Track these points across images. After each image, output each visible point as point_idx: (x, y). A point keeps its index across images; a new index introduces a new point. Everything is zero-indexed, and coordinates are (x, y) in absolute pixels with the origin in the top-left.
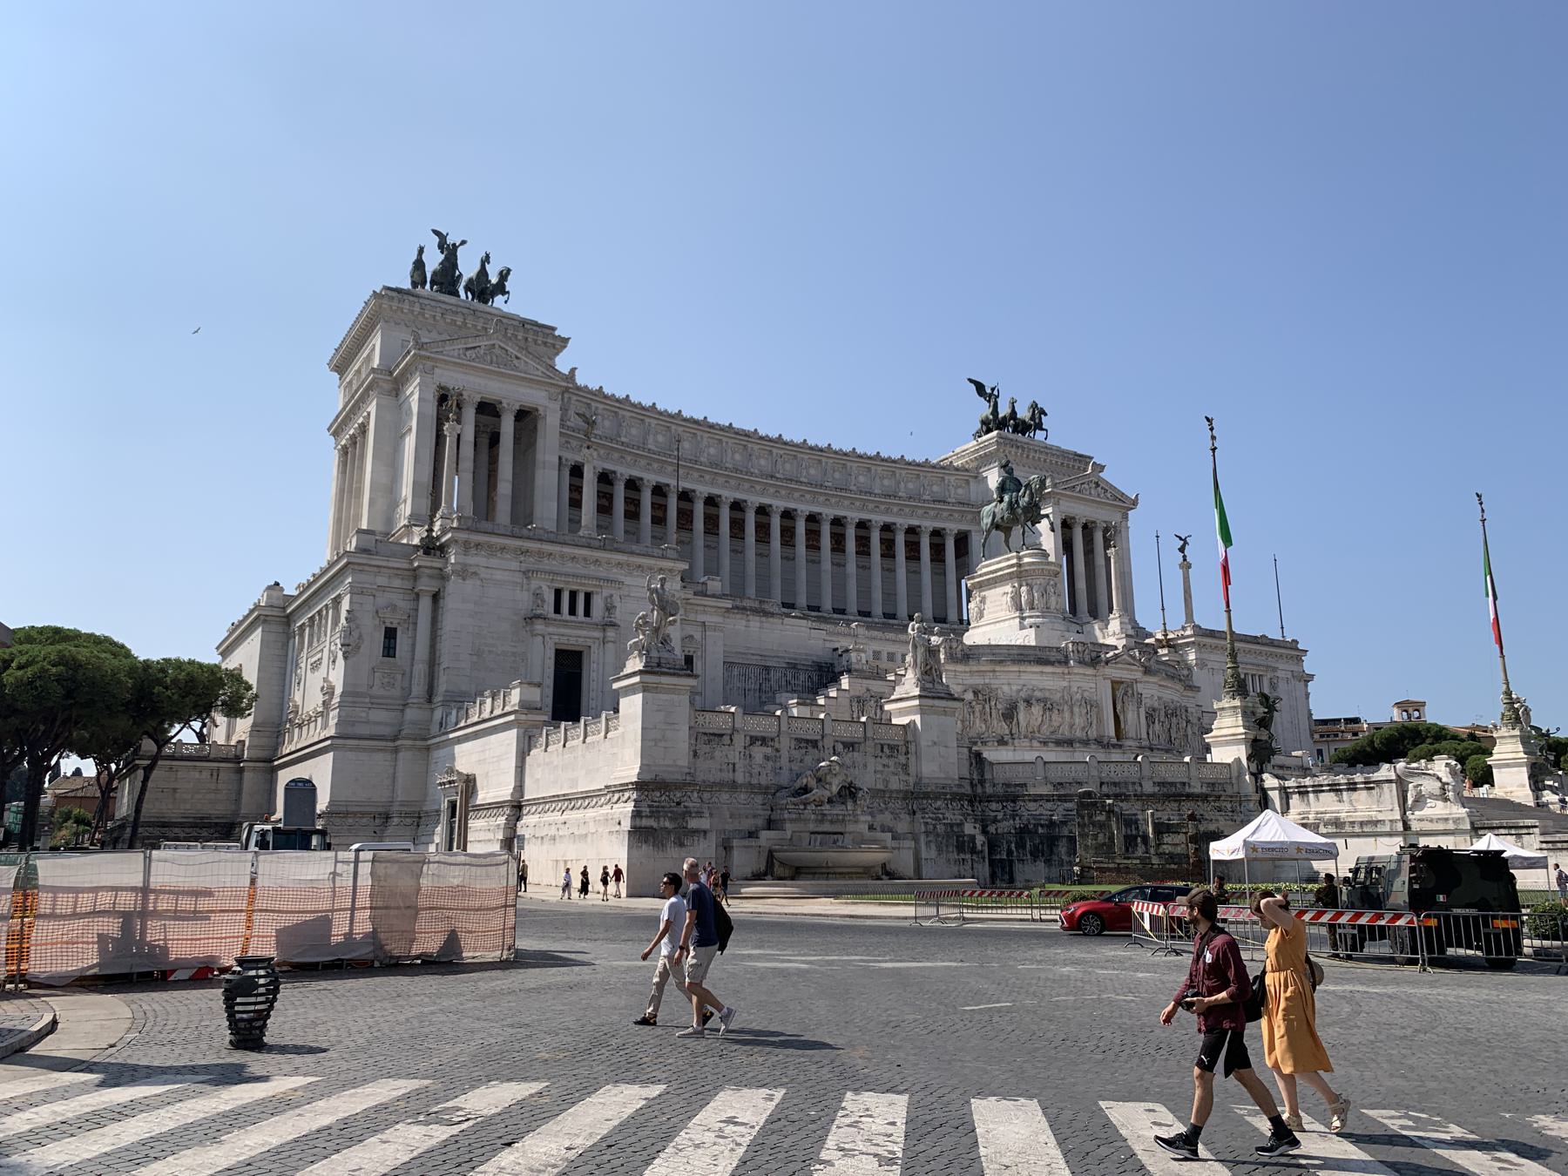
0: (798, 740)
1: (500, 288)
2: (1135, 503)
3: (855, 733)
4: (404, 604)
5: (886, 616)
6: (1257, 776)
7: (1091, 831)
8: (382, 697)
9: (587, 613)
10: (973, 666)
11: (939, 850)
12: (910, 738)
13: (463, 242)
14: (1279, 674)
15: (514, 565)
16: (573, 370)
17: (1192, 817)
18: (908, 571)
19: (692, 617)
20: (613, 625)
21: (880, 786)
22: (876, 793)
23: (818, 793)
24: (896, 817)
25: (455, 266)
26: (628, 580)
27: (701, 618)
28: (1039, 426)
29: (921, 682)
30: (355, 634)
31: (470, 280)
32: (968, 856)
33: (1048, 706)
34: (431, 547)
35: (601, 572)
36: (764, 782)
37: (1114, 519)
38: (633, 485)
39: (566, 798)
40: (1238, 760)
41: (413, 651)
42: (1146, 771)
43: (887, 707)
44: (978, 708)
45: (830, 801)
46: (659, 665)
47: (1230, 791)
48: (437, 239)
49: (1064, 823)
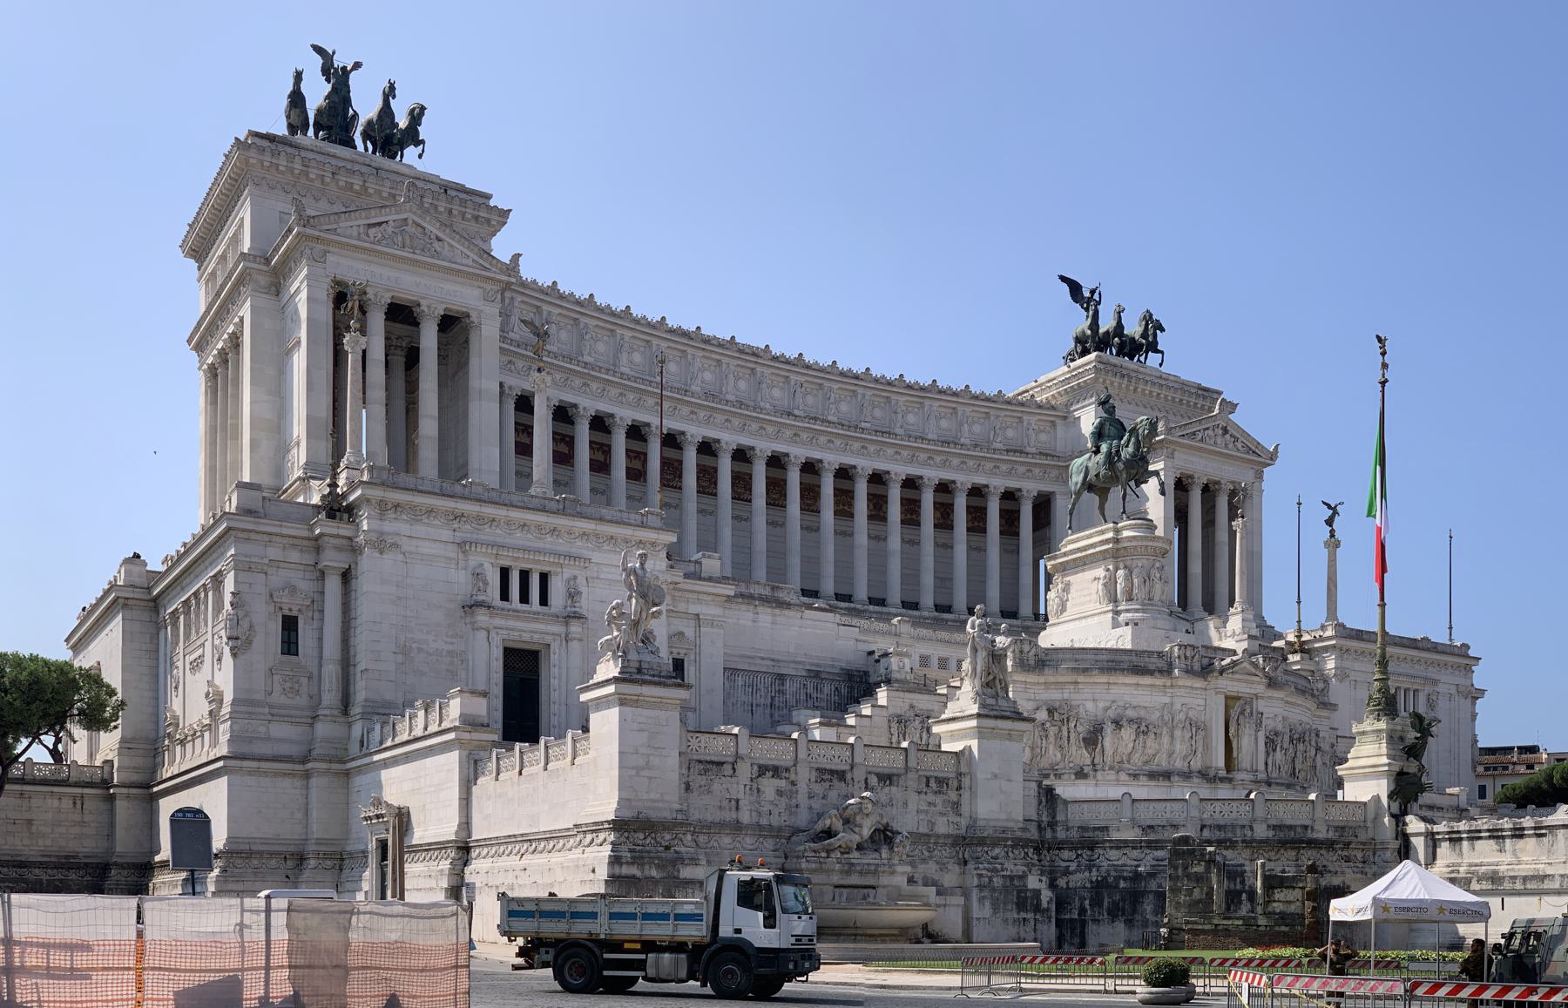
2: (1273, 456)
3: (893, 762)
4: (305, 585)
5: (938, 608)
6: (1399, 818)
7: (1185, 884)
8: (281, 707)
10: (1049, 676)
11: (995, 909)
12: (963, 769)
15: (446, 534)
17: (1312, 869)
18: (970, 548)
19: (681, 607)
20: (578, 617)
22: (917, 838)
23: (844, 838)
24: (943, 867)
26: (596, 557)
29: (980, 696)
30: (245, 624)
32: (1030, 916)
35: (562, 545)
36: (775, 821)
37: (1244, 477)
38: (600, 423)
39: (527, 839)
40: (1377, 799)
41: (321, 648)
42: (1260, 812)
43: (936, 729)
44: (1052, 731)
45: (860, 847)
47: (1362, 837)
49: (1152, 875)
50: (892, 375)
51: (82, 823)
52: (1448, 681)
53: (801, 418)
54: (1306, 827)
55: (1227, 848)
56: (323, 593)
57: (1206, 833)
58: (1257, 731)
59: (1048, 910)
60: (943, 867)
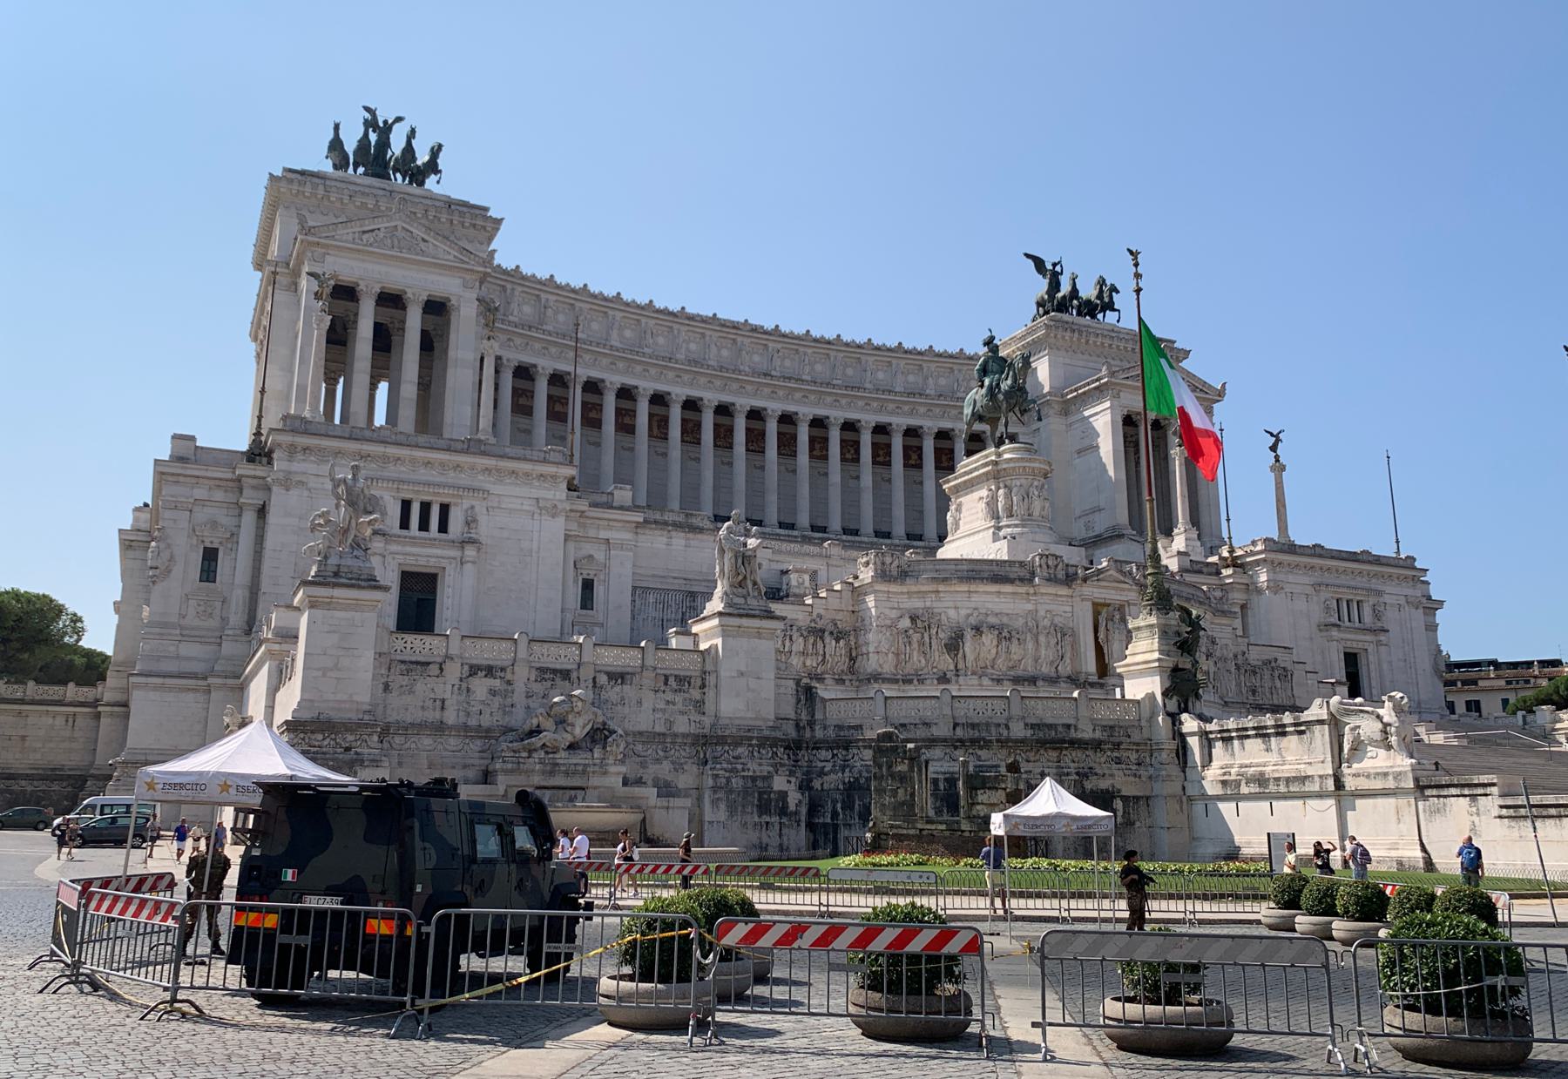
0: (542, 670)
1: (432, 167)
4: (226, 520)
5: (909, 536)
6: (1174, 718)
7: (890, 784)
8: (193, 629)
9: (443, 528)
10: (910, 586)
11: (732, 809)
12: (709, 667)
20: (472, 542)
24: (678, 767)
27: (603, 534)
28: (1109, 306)
30: (165, 555)
32: (775, 819)
33: (1005, 634)
35: (464, 479)
36: (486, 721)
40: (1152, 696)
42: (1016, 710)
44: (916, 637)
46: (336, 574)
47: (1136, 737)
50: (861, 339)
51: (72, 739)
52: (1394, 593)
53: (778, 378)
54: (1068, 726)
55: (981, 748)
59: (796, 813)
60: (678, 767)
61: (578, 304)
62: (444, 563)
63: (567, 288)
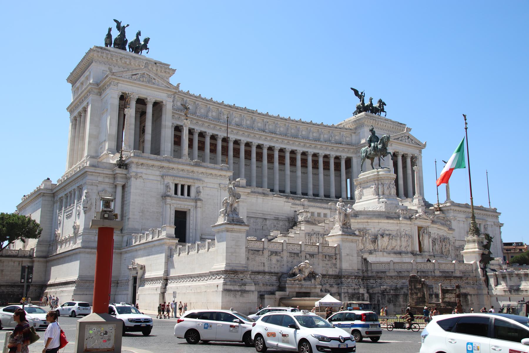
2: (425, 146)
3: (314, 250)
4: (109, 189)
9: (189, 195)
12: (337, 252)
13: (128, 25)
14: (488, 223)
15: (158, 173)
16: (178, 85)
17: (458, 287)
20: (200, 200)
21: (324, 273)
22: (324, 276)
24: (331, 286)
25: (124, 36)
26: (206, 180)
28: (383, 110)
29: (342, 228)
31: (132, 43)
34: (122, 164)
35: (195, 176)
36: (276, 270)
37: (416, 153)
42: (436, 267)
45: (304, 279)
46: (233, 220)
48: (116, 24)
49: (402, 288)
54: (452, 272)
56: (115, 192)
57: (419, 274)
58: (429, 238)
60: (331, 286)
61: (197, 102)
62: (190, 207)
63: (193, 96)
